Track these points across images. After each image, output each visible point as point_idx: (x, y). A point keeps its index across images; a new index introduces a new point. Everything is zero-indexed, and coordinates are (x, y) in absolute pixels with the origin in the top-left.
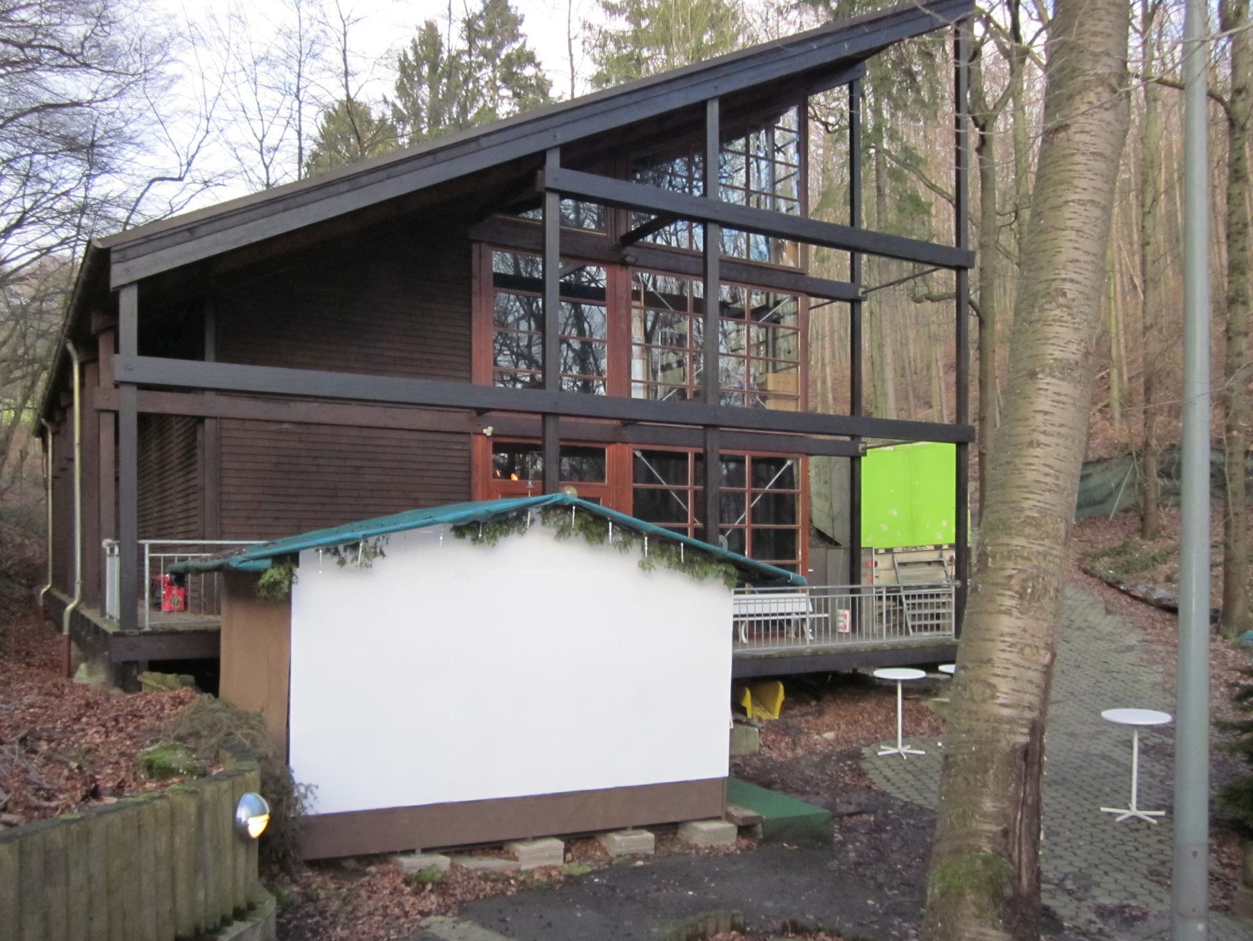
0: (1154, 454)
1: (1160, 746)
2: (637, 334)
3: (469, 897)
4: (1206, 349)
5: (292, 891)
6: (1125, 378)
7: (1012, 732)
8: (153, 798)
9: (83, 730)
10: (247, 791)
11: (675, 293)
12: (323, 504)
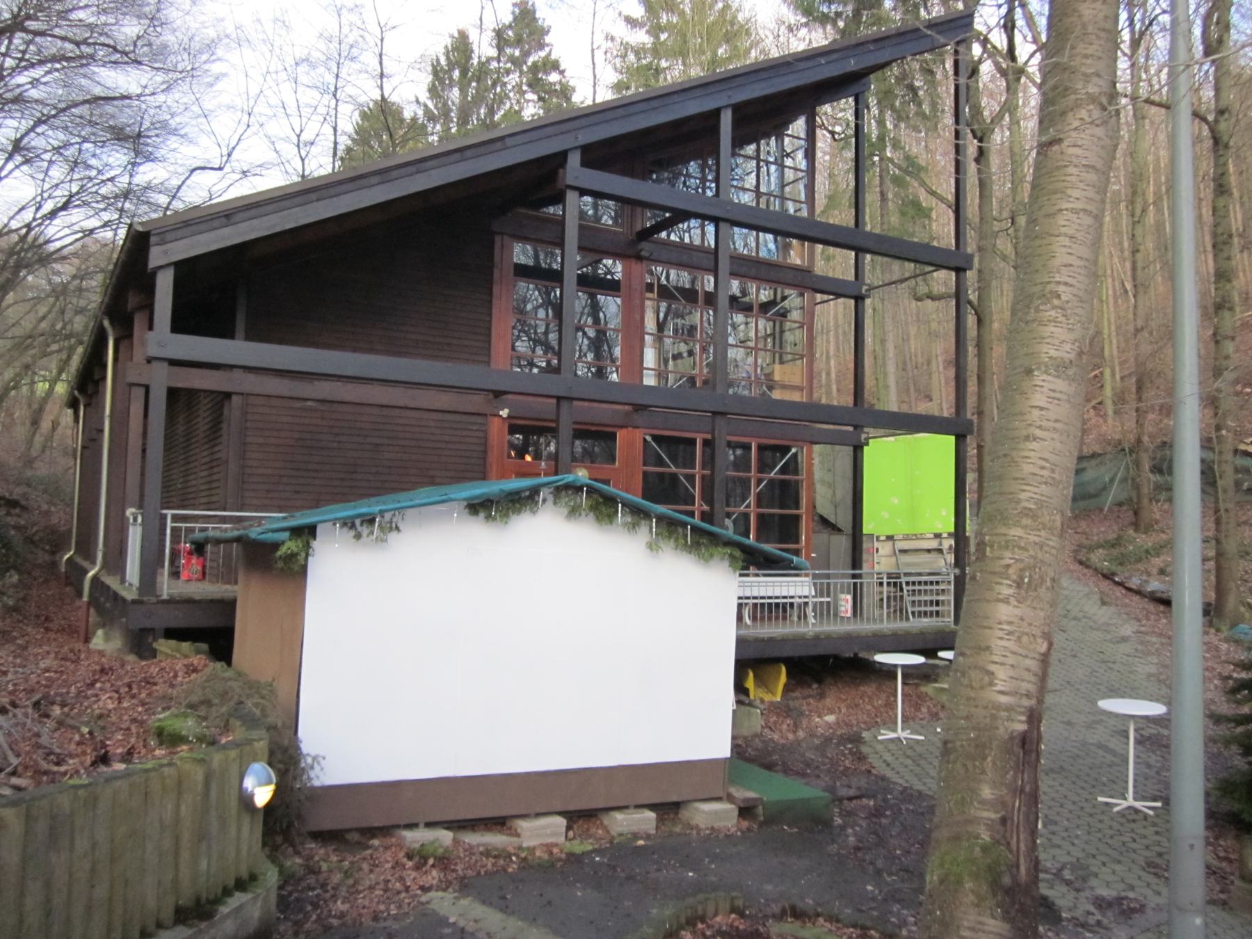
0: (1146, 450)
1: (1155, 738)
2: (650, 324)
3: (470, 873)
4: (1195, 351)
5: (295, 863)
6: (1118, 377)
7: (1010, 719)
8: (162, 766)
9: (96, 695)
10: (255, 760)
11: (687, 286)
12: (342, 479)
